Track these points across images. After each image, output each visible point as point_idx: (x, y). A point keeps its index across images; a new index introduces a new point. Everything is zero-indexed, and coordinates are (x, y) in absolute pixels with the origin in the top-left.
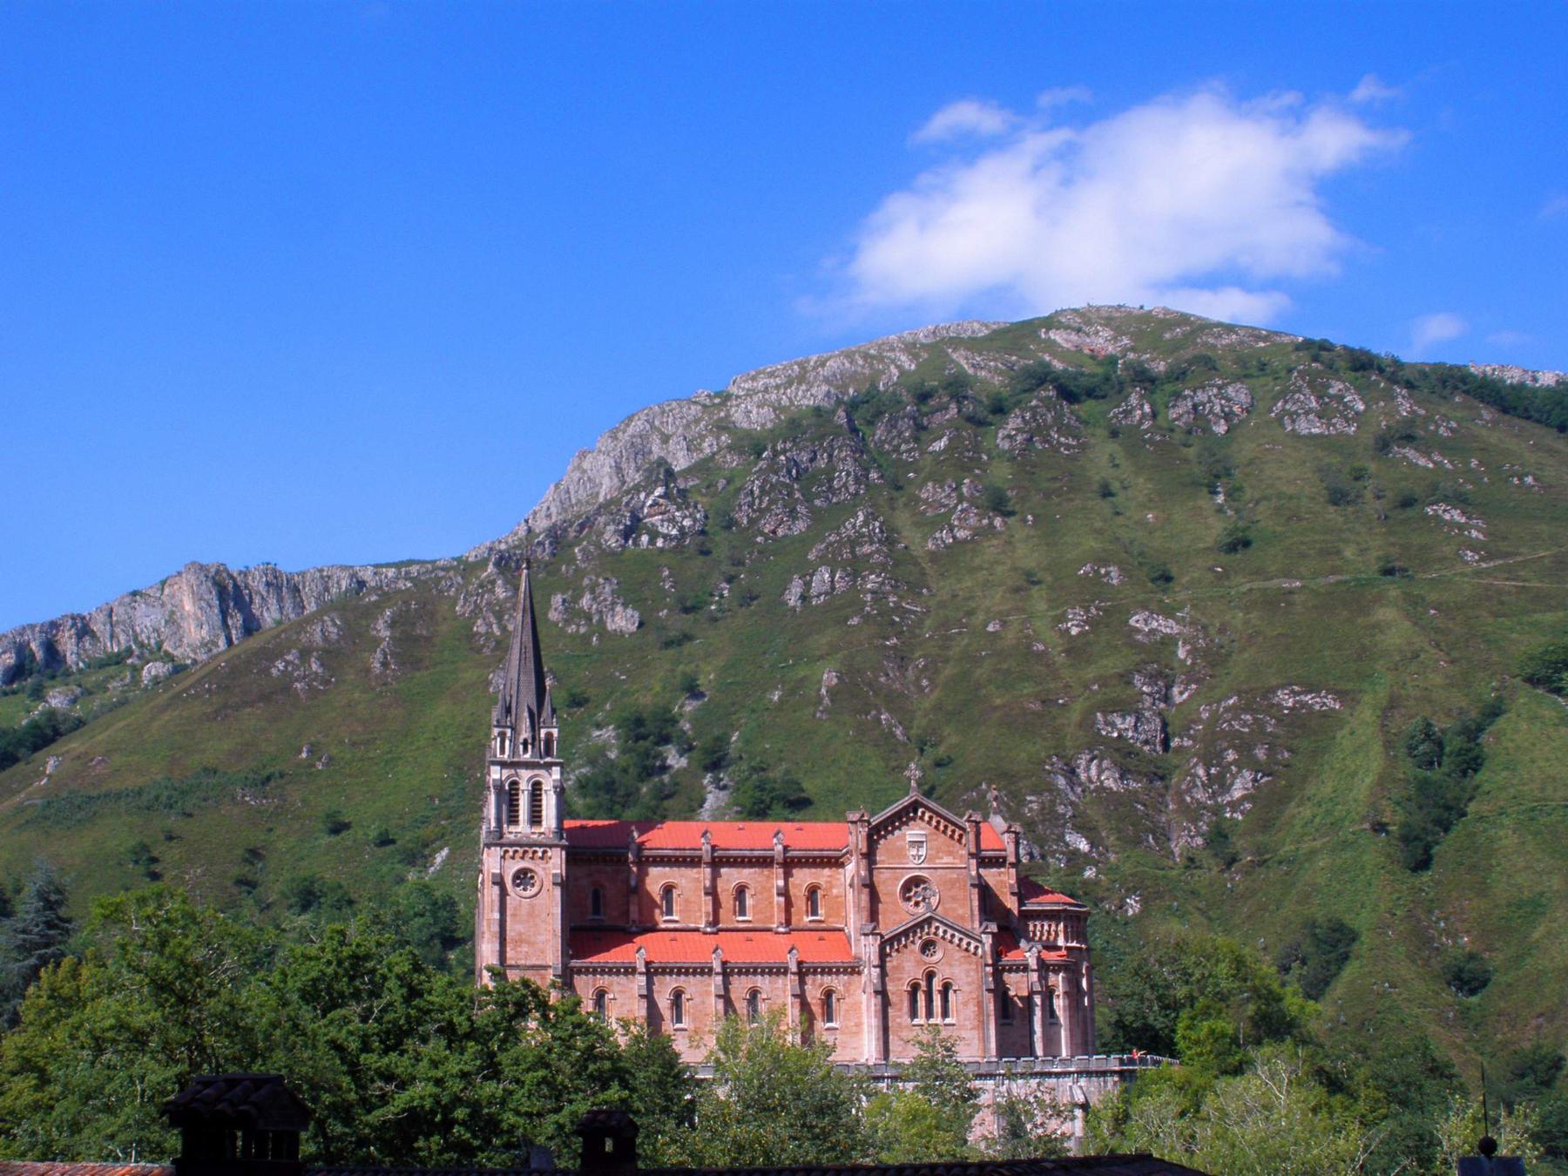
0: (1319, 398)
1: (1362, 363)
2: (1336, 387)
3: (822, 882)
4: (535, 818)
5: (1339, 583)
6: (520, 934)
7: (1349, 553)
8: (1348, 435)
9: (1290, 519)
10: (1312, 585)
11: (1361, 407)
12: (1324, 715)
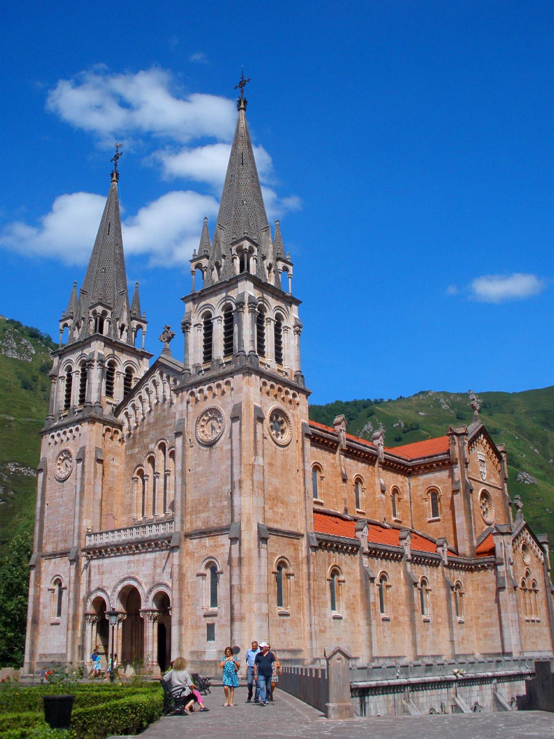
0: (17, 344)
1: (34, 335)
2: (24, 341)
3: (399, 485)
4: (279, 359)
5: (31, 422)
6: (276, 490)
7: (34, 410)
8: (28, 362)
9: (7, 390)
10: (19, 420)
11: (34, 352)
12: (29, 478)
